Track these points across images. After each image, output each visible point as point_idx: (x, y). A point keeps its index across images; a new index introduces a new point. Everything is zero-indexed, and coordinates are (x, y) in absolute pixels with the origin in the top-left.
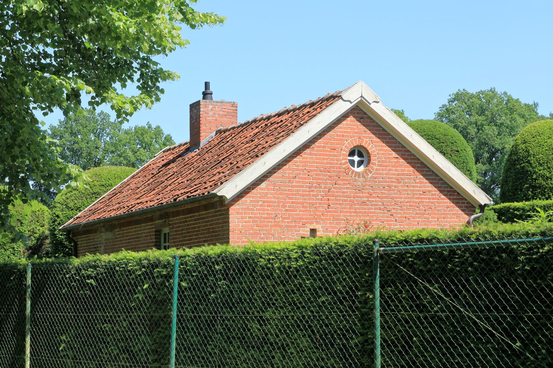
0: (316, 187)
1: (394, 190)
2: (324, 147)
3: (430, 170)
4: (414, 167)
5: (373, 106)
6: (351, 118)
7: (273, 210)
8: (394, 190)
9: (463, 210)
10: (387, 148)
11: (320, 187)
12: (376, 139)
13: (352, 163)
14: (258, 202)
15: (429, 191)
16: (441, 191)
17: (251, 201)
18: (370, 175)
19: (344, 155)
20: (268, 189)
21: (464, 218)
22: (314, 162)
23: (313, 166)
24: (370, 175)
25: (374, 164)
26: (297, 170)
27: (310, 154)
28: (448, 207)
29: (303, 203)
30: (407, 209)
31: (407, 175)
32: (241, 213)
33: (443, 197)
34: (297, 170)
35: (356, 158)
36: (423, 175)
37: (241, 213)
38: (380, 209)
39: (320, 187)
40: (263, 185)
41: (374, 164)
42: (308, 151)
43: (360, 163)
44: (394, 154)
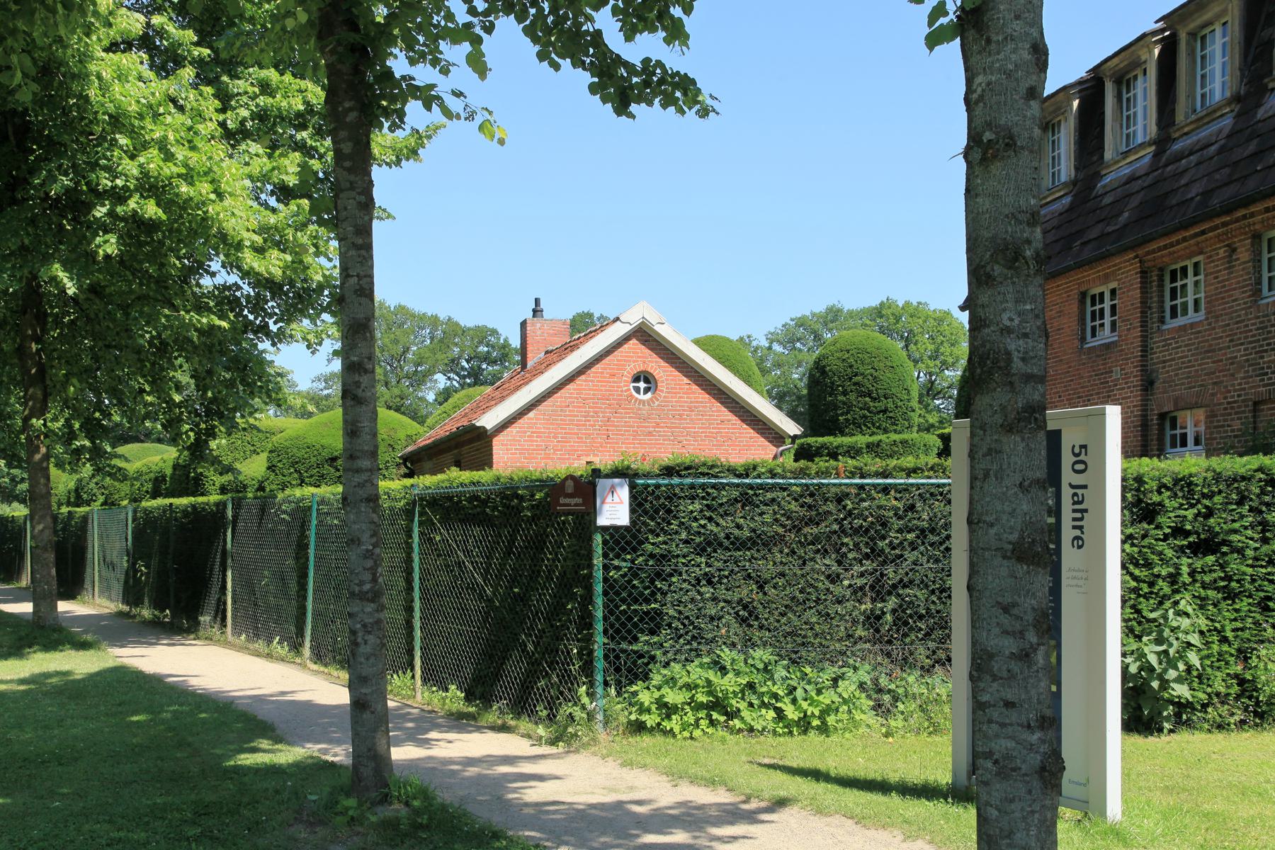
0: (593, 416)
1: (685, 419)
2: (602, 373)
3: (729, 397)
4: (709, 394)
5: (658, 328)
6: (634, 341)
7: (544, 441)
8: (685, 419)
9: (769, 441)
10: (677, 373)
11: (598, 416)
12: (663, 364)
13: (637, 390)
14: (525, 432)
15: (729, 420)
16: (743, 421)
17: (518, 432)
18: (657, 403)
19: (625, 381)
20: (537, 419)
21: (771, 450)
22: (590, 390)
23: (589, 394)
24: (657, 403)
25: (662, 391)
26: (570, 398)
27: (585, 381)
28: (751, 438)
29: (577, 434)
30: (702, 440)
31: (702, 402)
32: (507, 445)
33: (745, 426)
34: (570, 398)
35: (642, 385)
36: (721, 403)
37: (507, 445)
38: (670, 440)
39: (598, 416)
40: (531, 415)
41: (662, 391)
42: (583, 377)
43: (647, 390)
44: (686, 380)
